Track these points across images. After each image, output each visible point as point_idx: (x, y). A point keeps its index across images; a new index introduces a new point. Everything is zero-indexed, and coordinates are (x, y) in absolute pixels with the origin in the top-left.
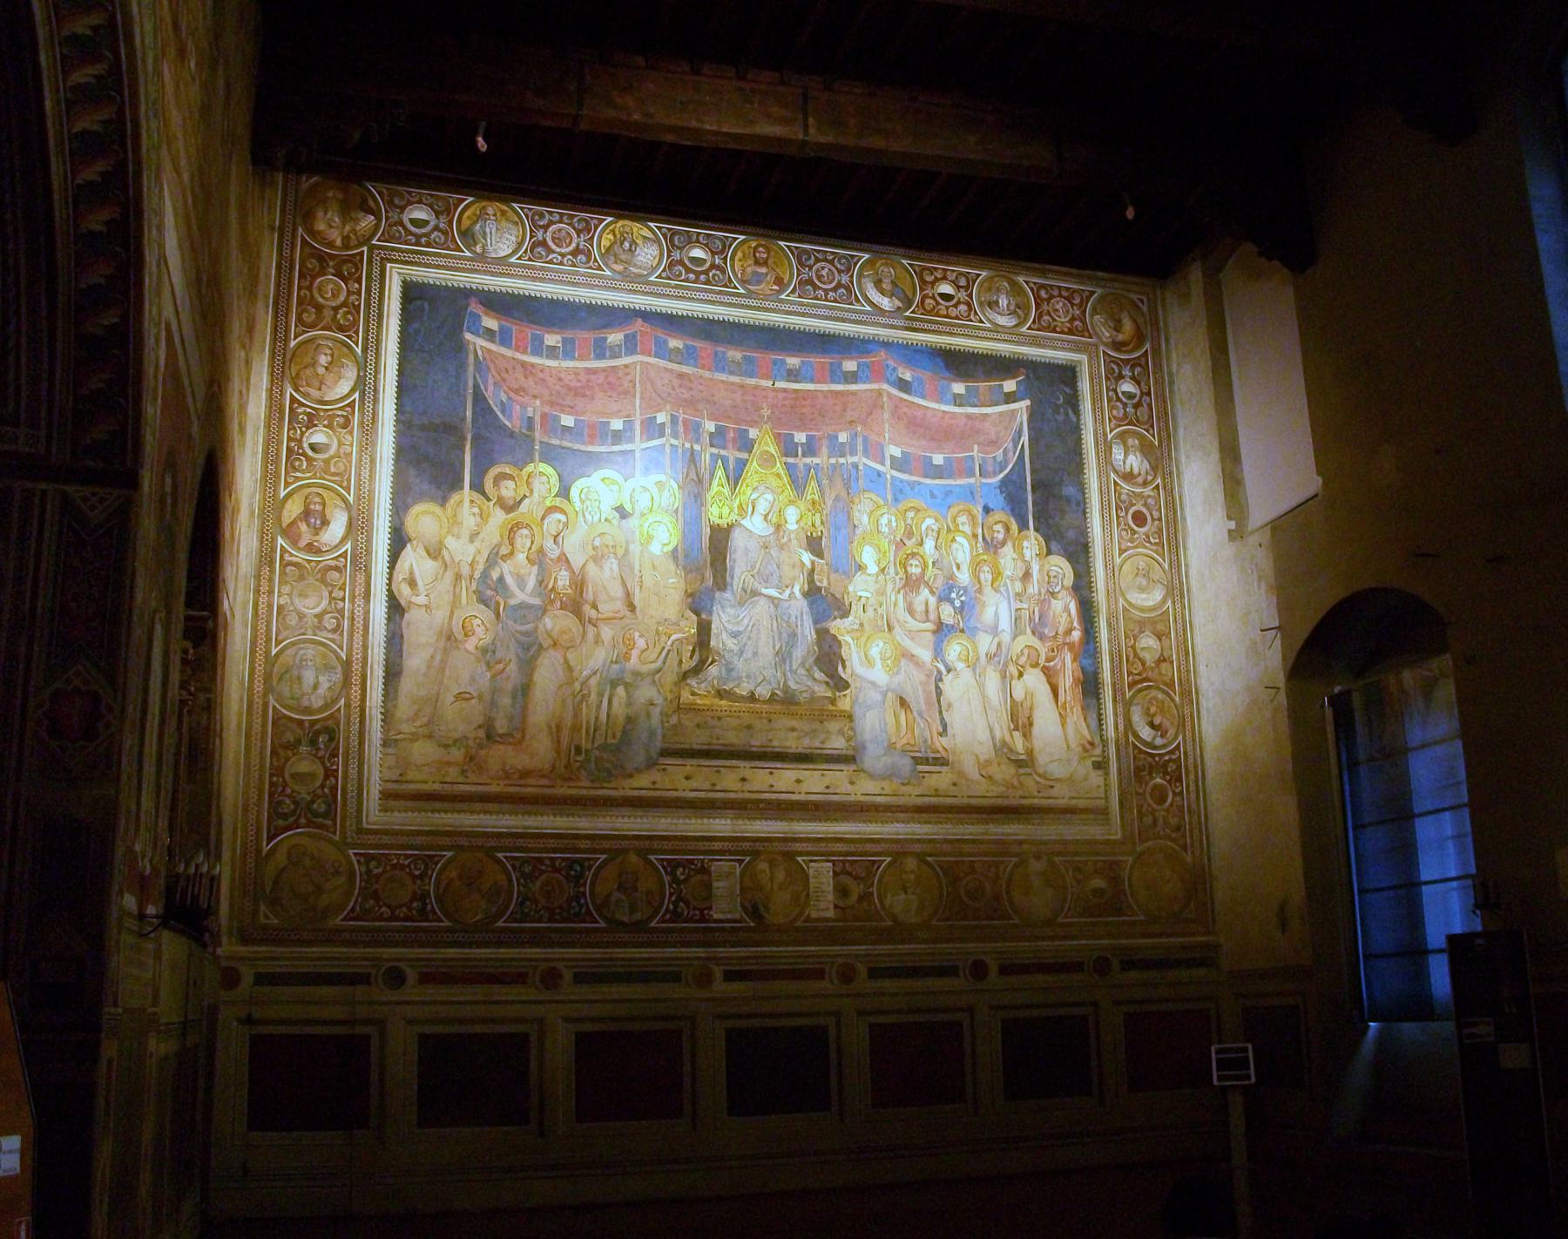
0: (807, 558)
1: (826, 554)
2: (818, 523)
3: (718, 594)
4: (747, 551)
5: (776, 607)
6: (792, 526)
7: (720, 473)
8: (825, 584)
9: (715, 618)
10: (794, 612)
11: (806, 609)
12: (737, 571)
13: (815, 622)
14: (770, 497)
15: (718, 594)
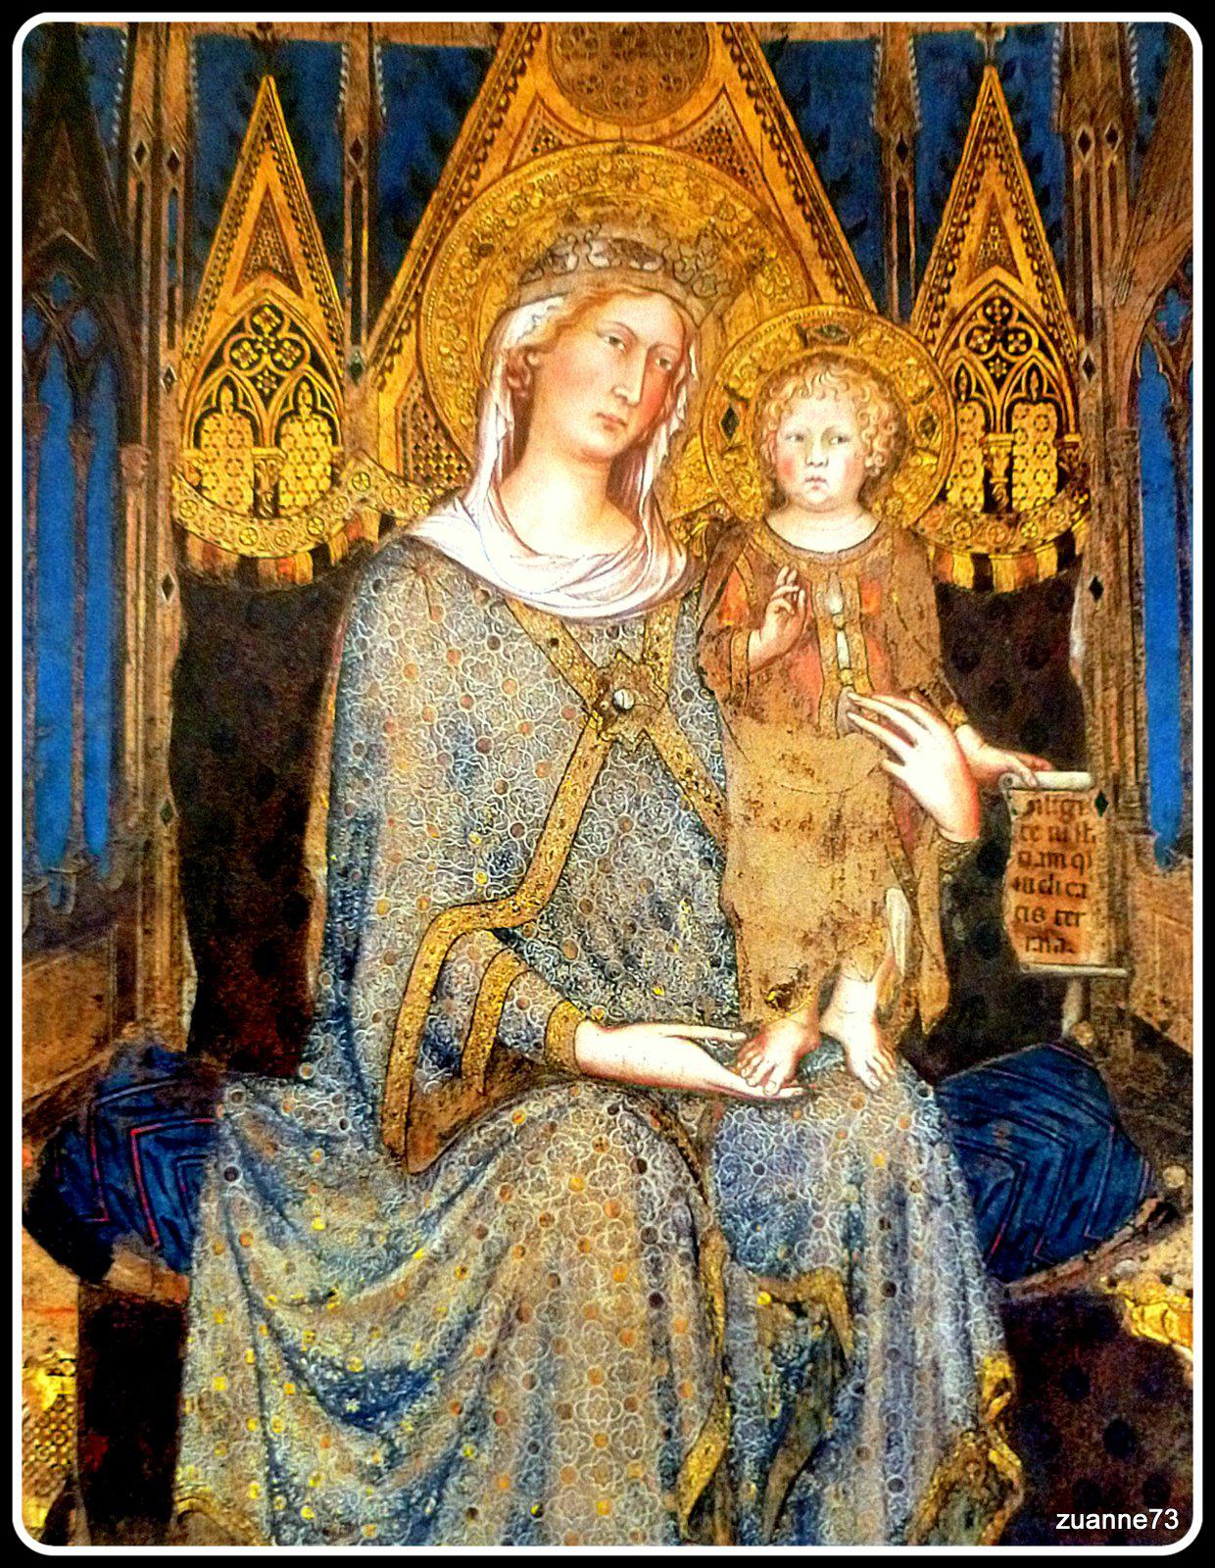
0: (941, 761)
1: (1100, 703)
2: (1035, 483)
3: (235, 1107)
4: (466, 753)
5: (694, 1156)
6: (826, 529)
7: (268, 178)
8: (1091, 956)
9: (211, 1278)
10: (829, 1190)
11: (932, 1167)
12: (390, 910)
13: (1004, 1255)
14: (650, 318)
15: (235, 1107)
